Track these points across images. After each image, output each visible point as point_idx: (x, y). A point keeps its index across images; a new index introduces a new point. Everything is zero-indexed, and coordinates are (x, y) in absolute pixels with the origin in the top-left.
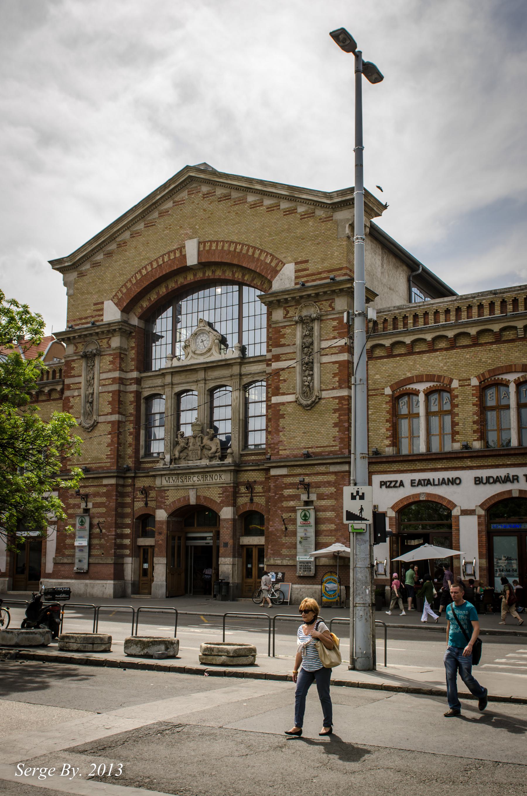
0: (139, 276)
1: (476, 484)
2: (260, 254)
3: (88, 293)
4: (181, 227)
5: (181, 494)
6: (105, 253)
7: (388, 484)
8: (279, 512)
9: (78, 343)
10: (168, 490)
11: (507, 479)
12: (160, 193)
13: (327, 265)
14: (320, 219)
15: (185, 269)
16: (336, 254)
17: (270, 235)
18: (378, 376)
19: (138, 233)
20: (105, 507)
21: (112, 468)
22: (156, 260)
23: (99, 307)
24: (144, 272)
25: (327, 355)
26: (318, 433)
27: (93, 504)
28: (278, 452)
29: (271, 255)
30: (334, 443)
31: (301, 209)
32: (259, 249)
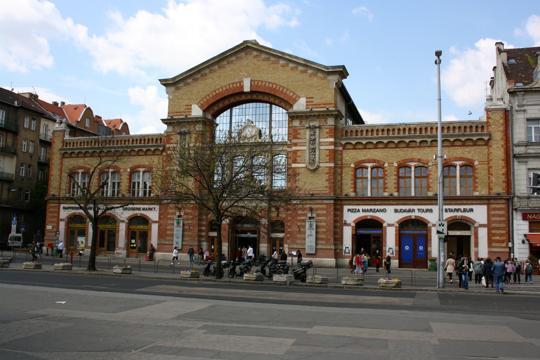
0: (214, 94)
1: (395, 212)
2: (287, 91)
3: (182, 99)
4: (240, 71)
6: (193, 79)
7: (352, 210)
8: (295, 222)
9: (175, 125)
11: (409, 211)
12: (229, 52)
13: (323, 101)
14: (320, 78)
15: (243, 93)
16: (328, 96)
17: (292, 82)
18: (347, 158)
19: (214, 71)
22: (225, 86)
23: (189, 107)
24: (217, 92)
25: (323, 145)
26: (317, 184)
29: (293, 92)
30: (326, 189)
31: (310, 71)
32: (286, 88)
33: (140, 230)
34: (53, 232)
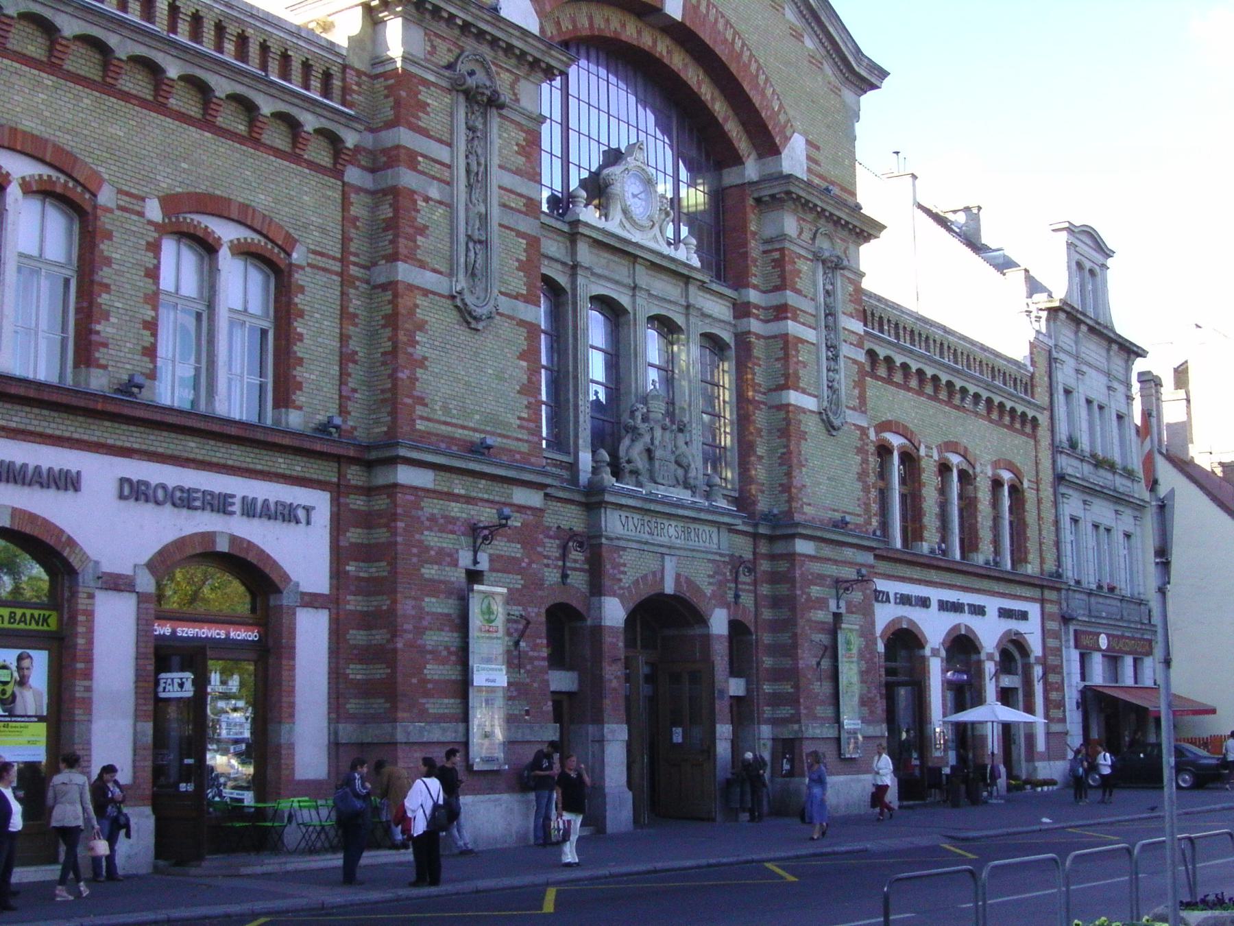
5: (652, 564)
10: (624, 549)
20: (520, 571)
21: (533, 460)
28: (802, 506)
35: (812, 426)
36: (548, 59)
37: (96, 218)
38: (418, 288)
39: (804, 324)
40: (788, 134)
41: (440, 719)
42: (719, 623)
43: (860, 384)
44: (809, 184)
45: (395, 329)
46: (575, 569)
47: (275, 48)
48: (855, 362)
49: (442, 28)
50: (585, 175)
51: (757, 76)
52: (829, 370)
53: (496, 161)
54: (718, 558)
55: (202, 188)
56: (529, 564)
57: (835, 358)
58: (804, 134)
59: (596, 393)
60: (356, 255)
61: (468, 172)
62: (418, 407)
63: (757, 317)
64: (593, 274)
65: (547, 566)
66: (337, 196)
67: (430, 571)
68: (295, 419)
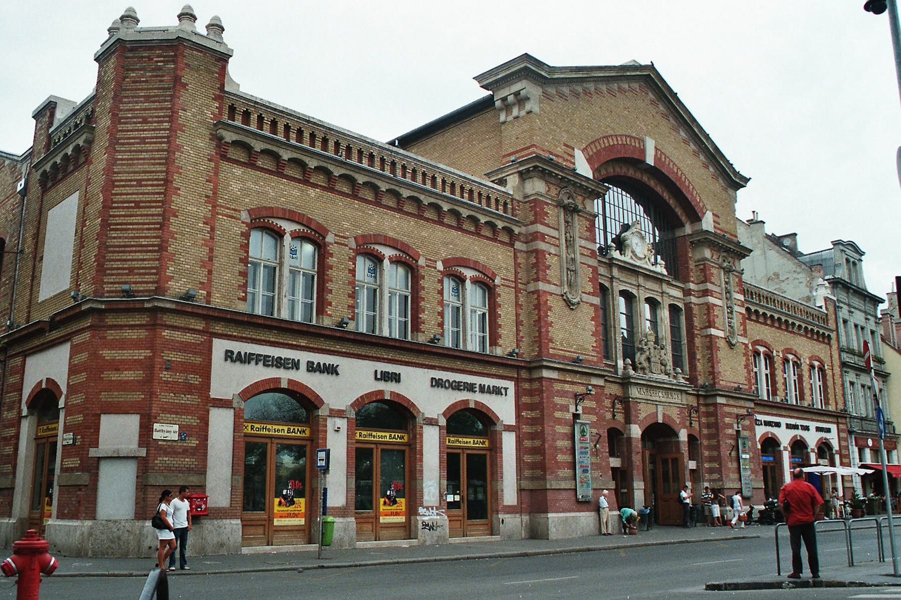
5: (651, 409)
10: (640, 403)
20: (596, 414)
27: (583, 408)
33: (469, 452)
34: (186, 452)
35: (722, 344)
36: (597, 189)
37: (418, 271)
38: (548, 292)
39: (716, 298)
40: (704, 211)
41: (565, 479)
42: (683, 436)
43: (743, 324)
44: (715, 234)
45: (539, 310)
46: (618, 412)
47: (484, 194)
48: (741, 313)
49: (553, 180)
50: (614, 236)
51: (689, 187)
52: (728, 318)
53: (577, 235)
54: (681, 406)
55: (459, 255)
56: (599, 410)
57: (731, 312)
58: (712, 210)
59: (623, 333)
60: (521, 279)
61: (566, 241)
62: (550, 344)
63: (694, 295)
64: (620, 281)
65: (607, 411)
66: (512, 254)
67: (558, 414)
68: (499, 351)
